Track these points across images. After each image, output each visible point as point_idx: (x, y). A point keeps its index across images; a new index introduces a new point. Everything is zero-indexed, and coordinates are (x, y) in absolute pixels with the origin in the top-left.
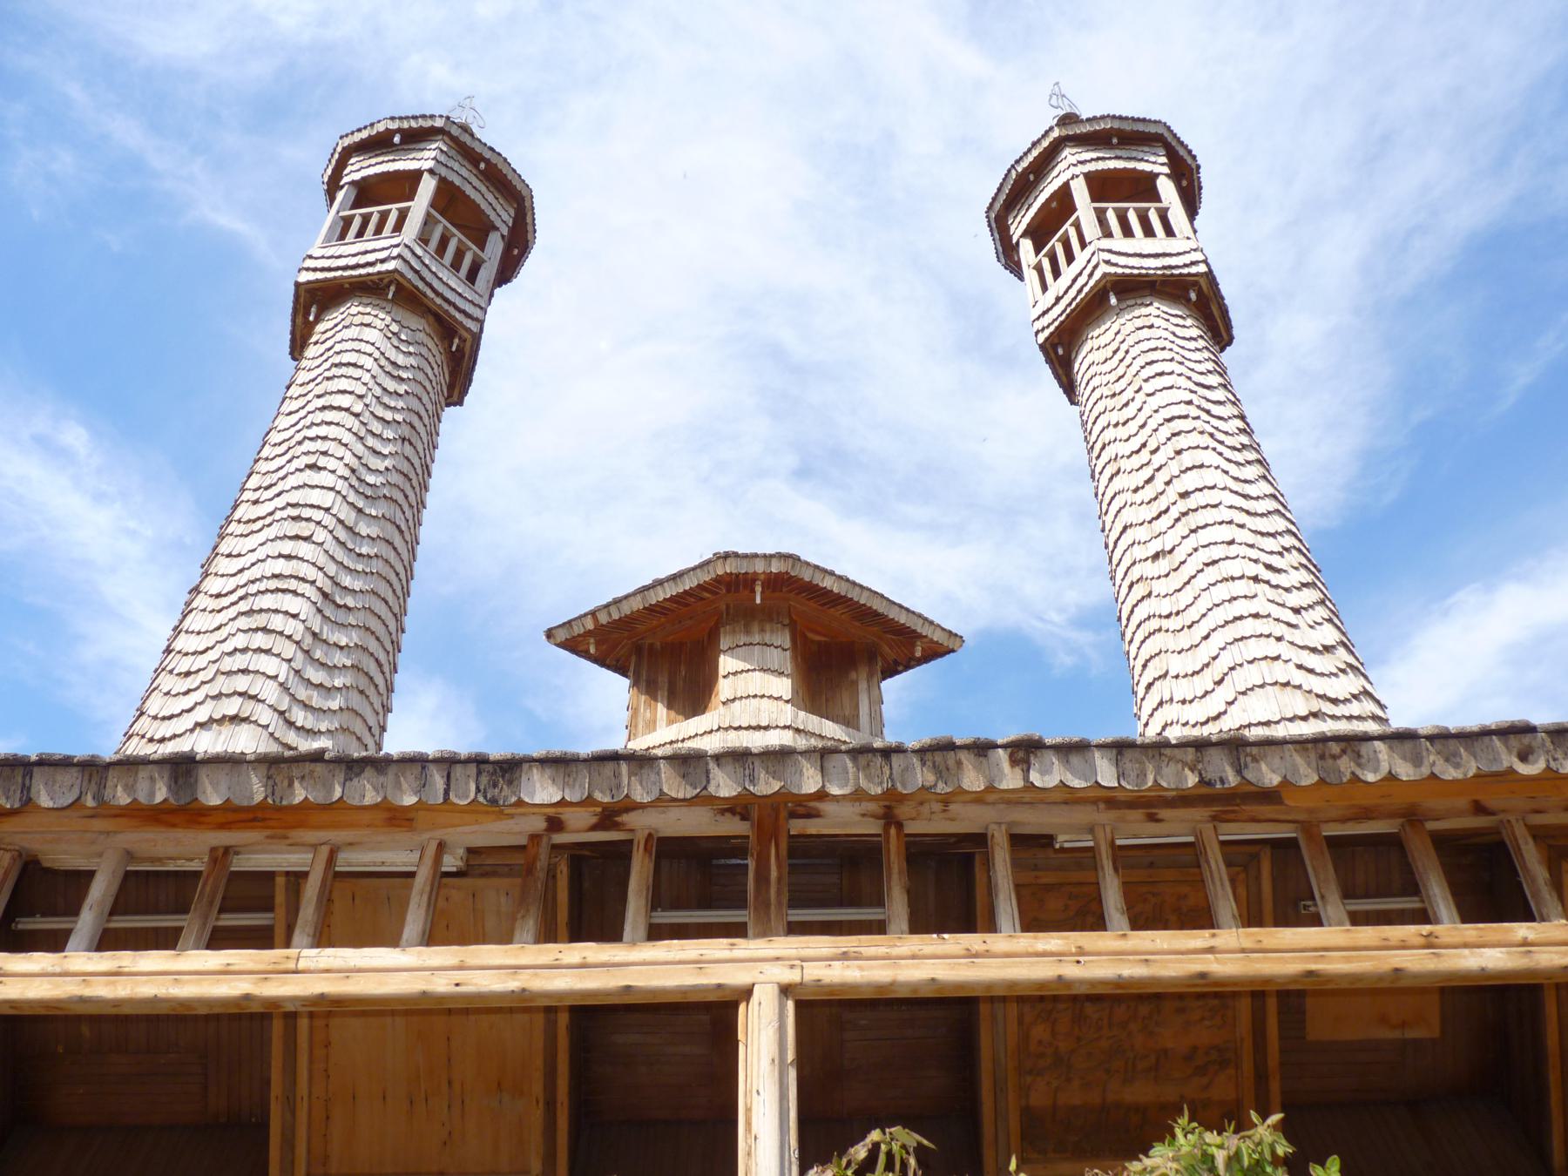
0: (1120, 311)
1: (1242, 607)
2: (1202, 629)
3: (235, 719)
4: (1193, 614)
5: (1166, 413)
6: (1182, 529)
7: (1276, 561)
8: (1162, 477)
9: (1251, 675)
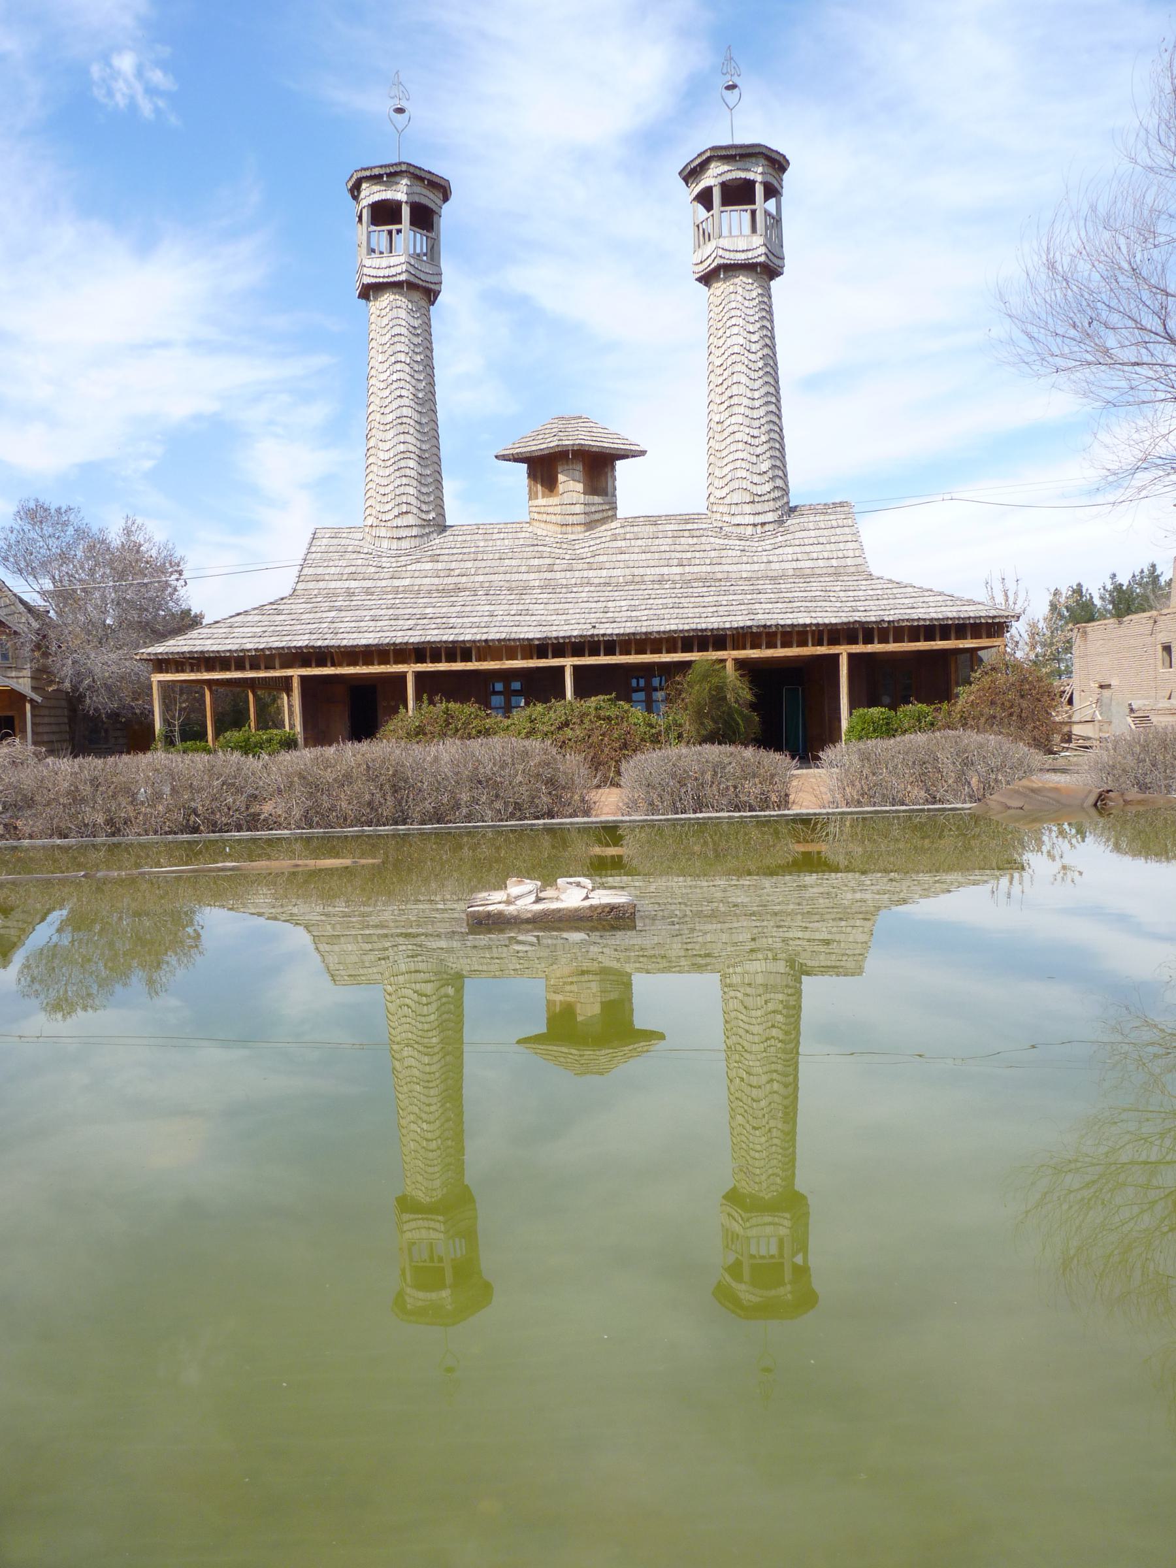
0: (725, 280)
1: (740, 455)
3: (407, 513)
4: (724, 453)
5: (730, 351)
6: (727, 414)
7: (756, 432)
8: (725, 386)
9: (735, 484)
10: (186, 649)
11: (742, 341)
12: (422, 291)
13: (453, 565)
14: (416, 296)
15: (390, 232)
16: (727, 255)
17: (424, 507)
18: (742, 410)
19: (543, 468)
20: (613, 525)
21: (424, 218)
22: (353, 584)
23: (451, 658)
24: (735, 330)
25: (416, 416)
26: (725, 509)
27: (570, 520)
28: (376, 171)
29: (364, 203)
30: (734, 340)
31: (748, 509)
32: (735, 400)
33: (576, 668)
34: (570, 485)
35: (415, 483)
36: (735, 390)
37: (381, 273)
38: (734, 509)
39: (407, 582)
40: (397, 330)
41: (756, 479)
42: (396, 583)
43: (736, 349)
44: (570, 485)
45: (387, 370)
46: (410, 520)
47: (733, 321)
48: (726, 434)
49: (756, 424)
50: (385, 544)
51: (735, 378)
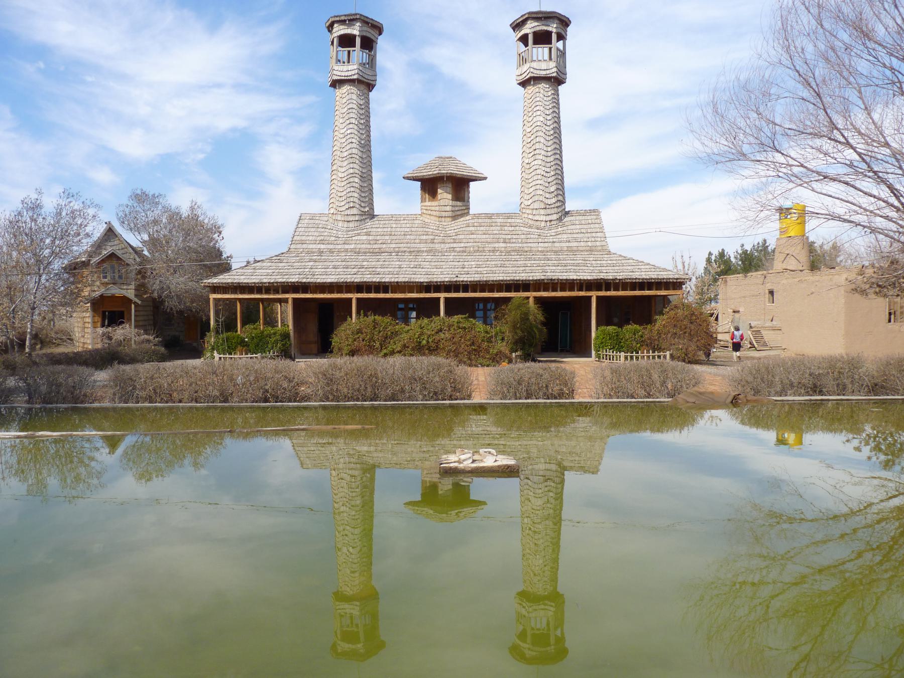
0: (534, 85)
1: (539, 182)
6: (532, 159)
7: (548, 170)
9: (536, 198)
10: (229, 281)
11: (542, 119)
12: (366, 84)
13: (378, 238)
14: (362, 87)
15: (349, 52)
16: (535, 72)
17: (363, 205)
18: (541, 157)
19: (430, 185)
20: (467, 218)
21: (368, 44)
22: (322, 246)
23: (377, 291)
24: (539, 113)
25: (360, 154)
26: (530, 212)
27: (444, 214)
28: (343, 18)
29: (335, 35)
30: (538, 118)
31: (542, 212)
33: (446, 299)
34: (445, 196)
35: (358, 191)
36: (537, 146)
37: (343, 74)
39: (352, 246)
40: (351, 106)
41: (548, 195)
42: (347, 247)
43: (539, 124)
44: (445, 196)
45: (344, 128)
46: (355, 211)
47: (538, 108)
48: (532, 170)
49: (549, 165)
50: (340, 224)
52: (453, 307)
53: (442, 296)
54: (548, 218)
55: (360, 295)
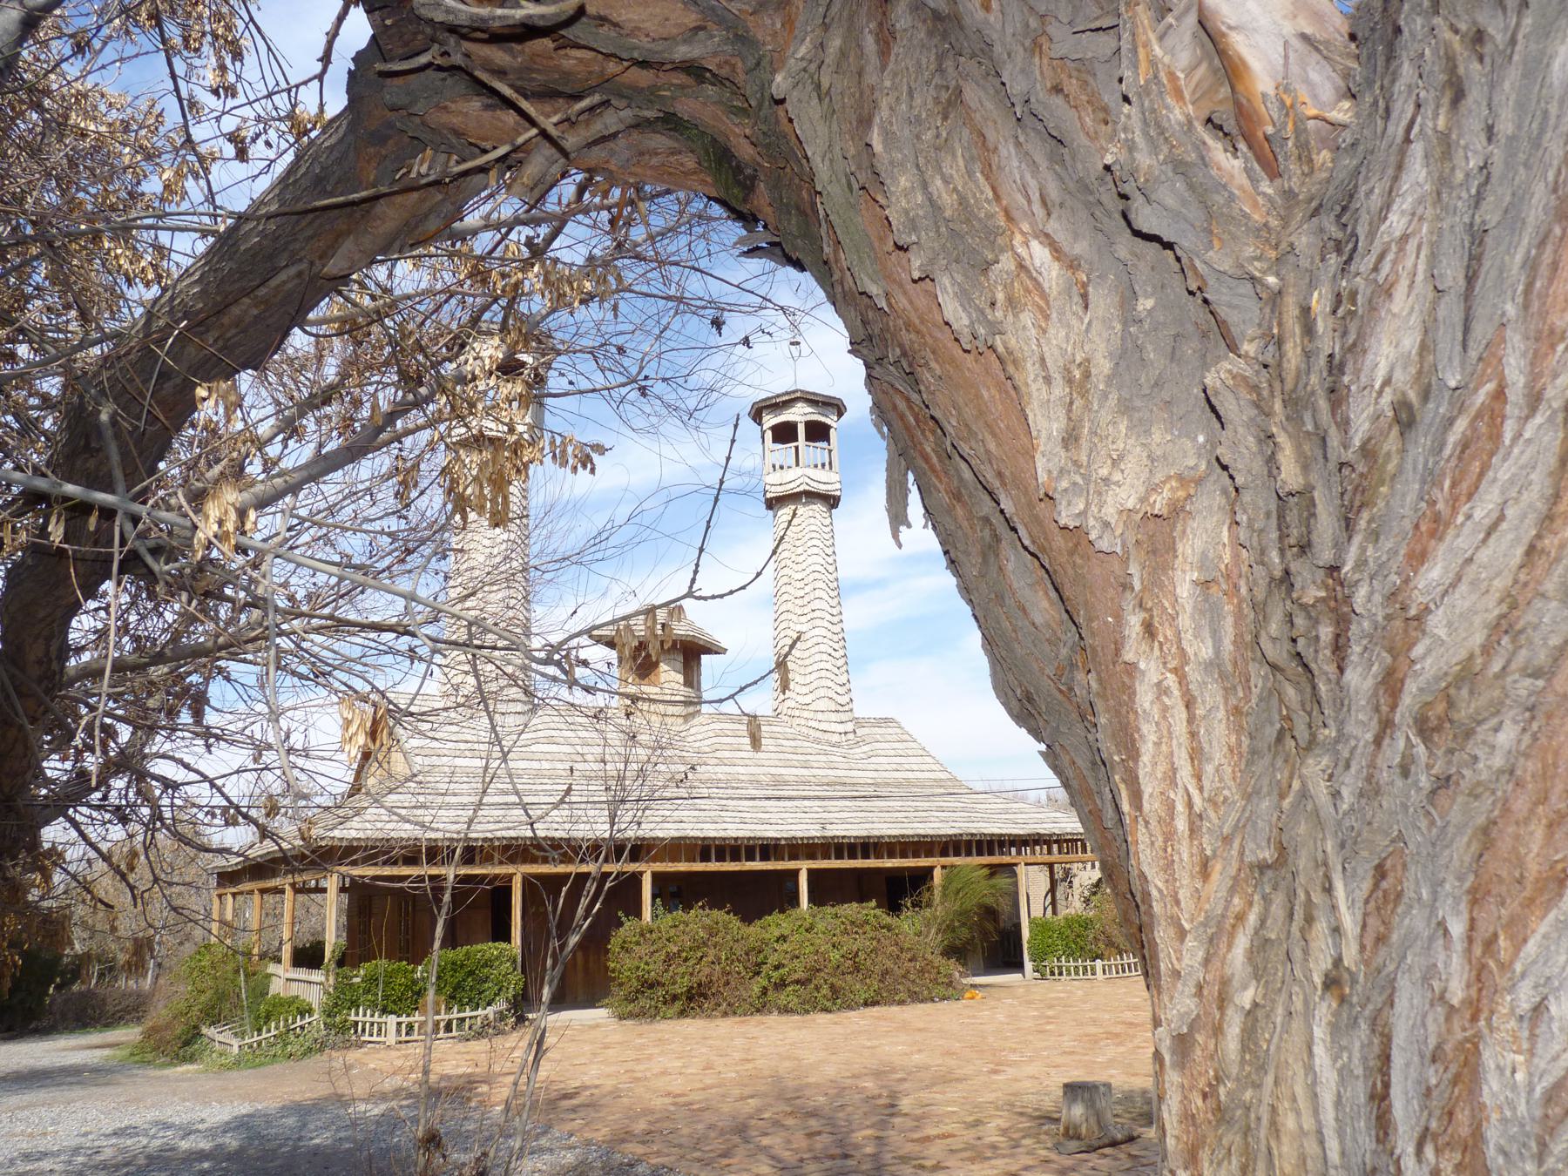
1: (822, 665)
2: (810, 669)
4: (807, 662)
5: (813, 568)
6: (810, 625)
7: (836, 646)
9: (822, 692)
24: (815, 550)
26: (811, 715)
31: (834, 717)
32: (817, 614)
34: (669, 676)
36: (817, 604)
38: (820, 716)
44: (669, 676)
51: (818, 593)
52: (827, 889)
53: (804, 866)
54: (841, 728)
55: (660, 867)
